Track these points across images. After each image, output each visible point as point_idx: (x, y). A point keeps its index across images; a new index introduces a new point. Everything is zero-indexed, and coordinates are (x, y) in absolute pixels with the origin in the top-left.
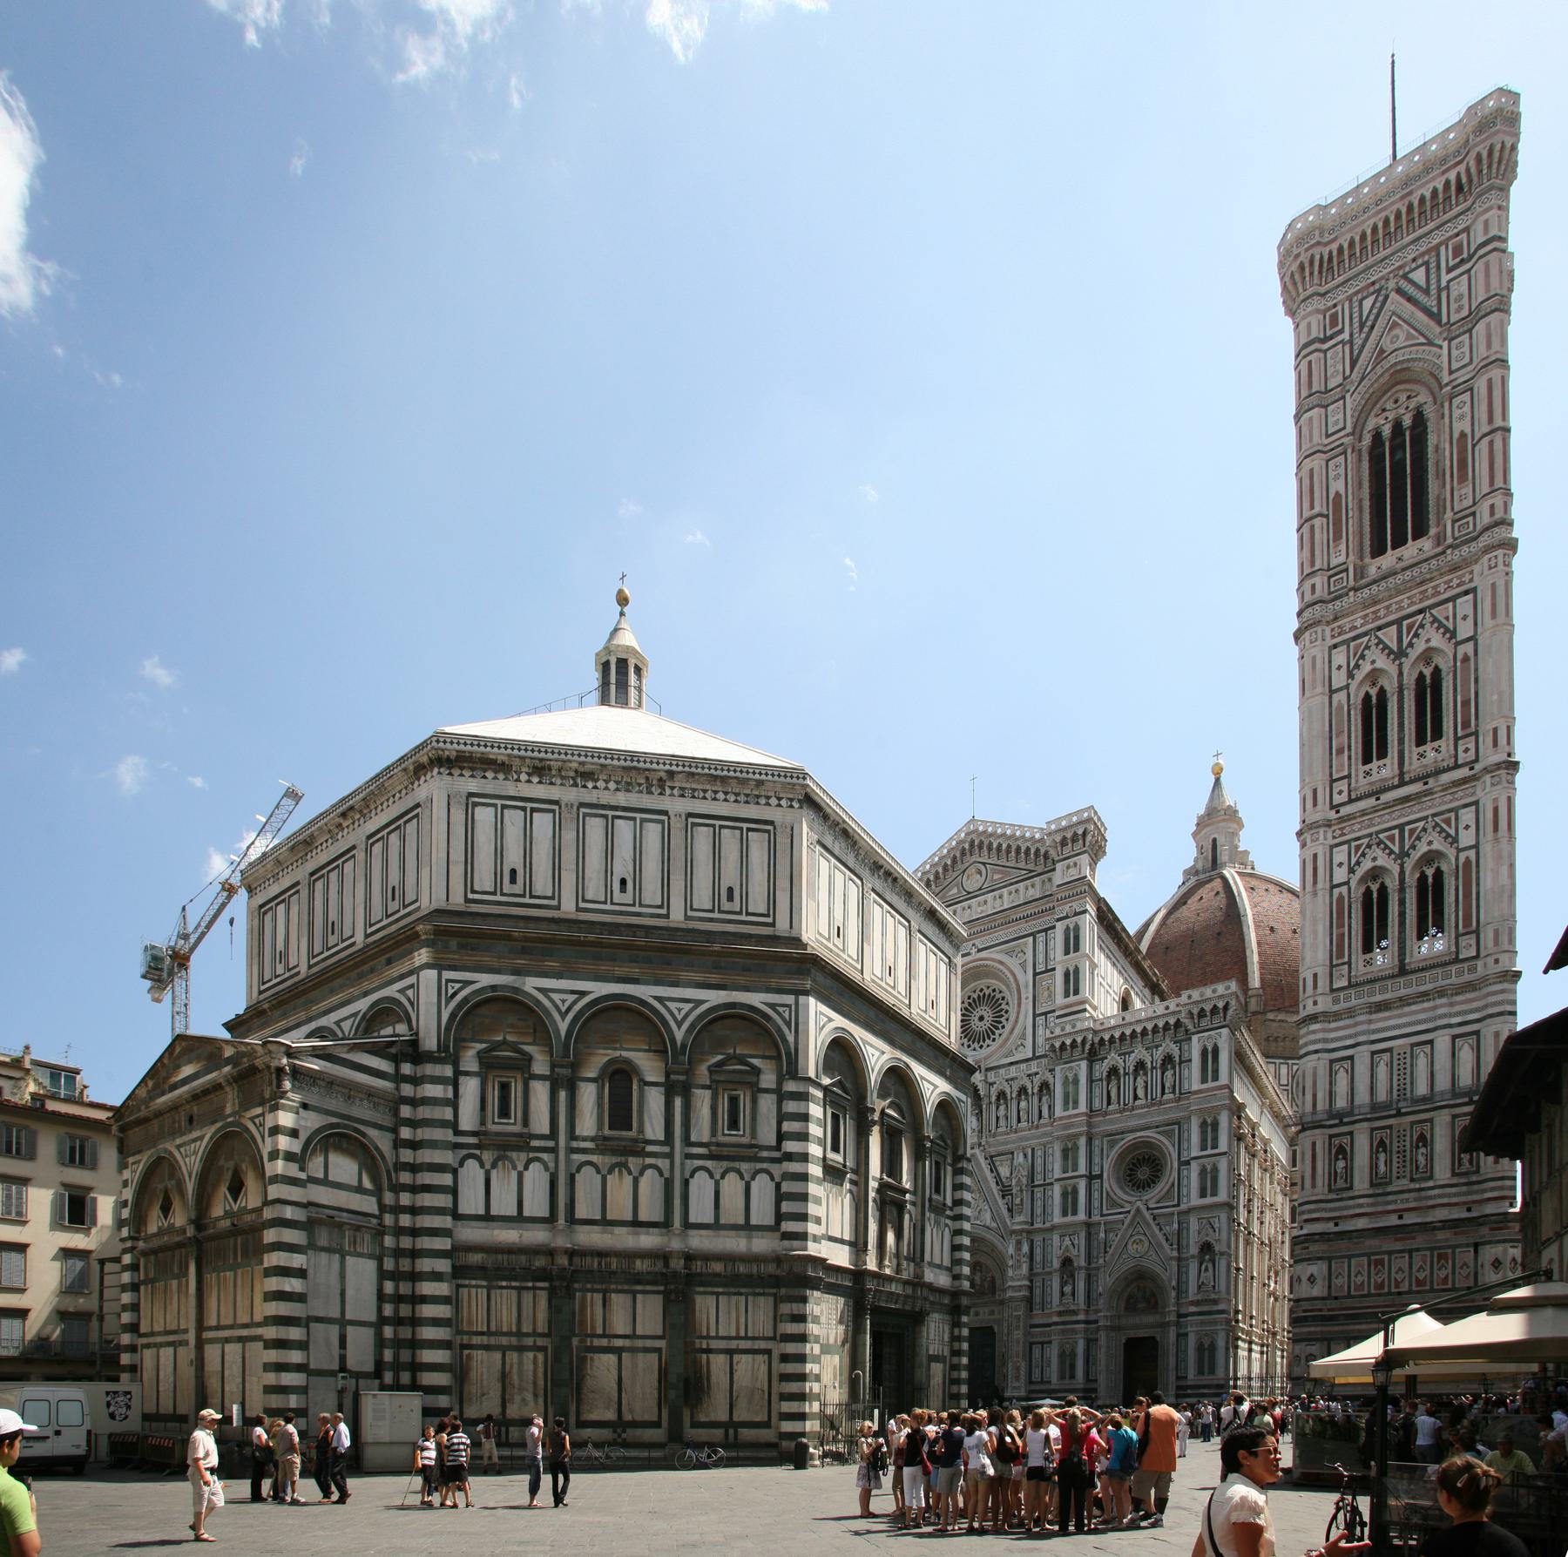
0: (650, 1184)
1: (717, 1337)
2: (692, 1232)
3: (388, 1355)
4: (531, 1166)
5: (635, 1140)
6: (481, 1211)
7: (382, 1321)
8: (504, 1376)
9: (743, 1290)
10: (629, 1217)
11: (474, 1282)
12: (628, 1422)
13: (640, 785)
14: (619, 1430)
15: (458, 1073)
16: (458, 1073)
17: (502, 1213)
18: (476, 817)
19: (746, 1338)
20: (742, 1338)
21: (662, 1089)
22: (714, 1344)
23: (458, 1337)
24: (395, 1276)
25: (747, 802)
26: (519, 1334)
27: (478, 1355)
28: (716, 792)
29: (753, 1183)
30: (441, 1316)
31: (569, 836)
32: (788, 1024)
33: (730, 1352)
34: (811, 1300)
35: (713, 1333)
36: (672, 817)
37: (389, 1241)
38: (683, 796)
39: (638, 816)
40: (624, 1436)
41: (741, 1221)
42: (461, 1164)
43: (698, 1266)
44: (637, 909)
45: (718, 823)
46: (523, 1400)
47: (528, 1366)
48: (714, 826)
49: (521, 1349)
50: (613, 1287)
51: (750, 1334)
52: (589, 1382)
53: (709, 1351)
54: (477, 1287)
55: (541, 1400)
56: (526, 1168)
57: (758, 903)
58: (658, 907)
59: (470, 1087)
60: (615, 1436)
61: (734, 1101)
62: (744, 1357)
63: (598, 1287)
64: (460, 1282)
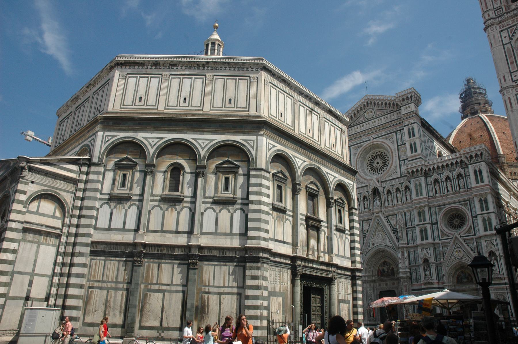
0: (185, 214)
1: (214, 286)
2: (203, 236)
3: (54, 291)
4: (131, 207)
5: (180, 196)
6: (107, 227)
7: (54, 274)
8: (107, 303)
9: (228, 264)
10: (174, 229)
11: (99, 258)
12: (166, 327)
13: (195, 67)
14: (160, 332)
15: (105, 170)
16: (105, 170)
17: (116, 228)
18: (129, 81)
19: (228, 287)
20: (226, 287)
21: (194, 175)
22: (212, 290)
23: (88, 283)
24: (65, 254)
25: (239, 70)
26: (117, 282)
27: (96, 291)
28: (226, 68)
29: (234, 214)
30: (80, 272)
31: (165, 84)
32: (253, 148)
33: (220, 294)
34: (262, 268)
35: (211, 284)
36: (207, 77)
37: (63, 239)
38: (212, 69)
39: (193, 77)
40: (162, 334)
41: (228, 231)
42: (101, 207)
43: (205, 253)
44: (190, 108)
45: (226, 77)
46: (114, 314)
47: (119, 298)
48: (224, 79)
49: (116, 289)
50: (163, 261)
51: (230, 285)
52: (147, 306)
53: (209, 293)
54: (100, 260)
55: (122, 314)
56: (129, 208)
57: (242, 103)
58: (199, 107)
59: (110, 175)
60: (158, 334)
61: (227, 179)
62: (227, 296)
63: (156, 261)
64: (92, 257)
